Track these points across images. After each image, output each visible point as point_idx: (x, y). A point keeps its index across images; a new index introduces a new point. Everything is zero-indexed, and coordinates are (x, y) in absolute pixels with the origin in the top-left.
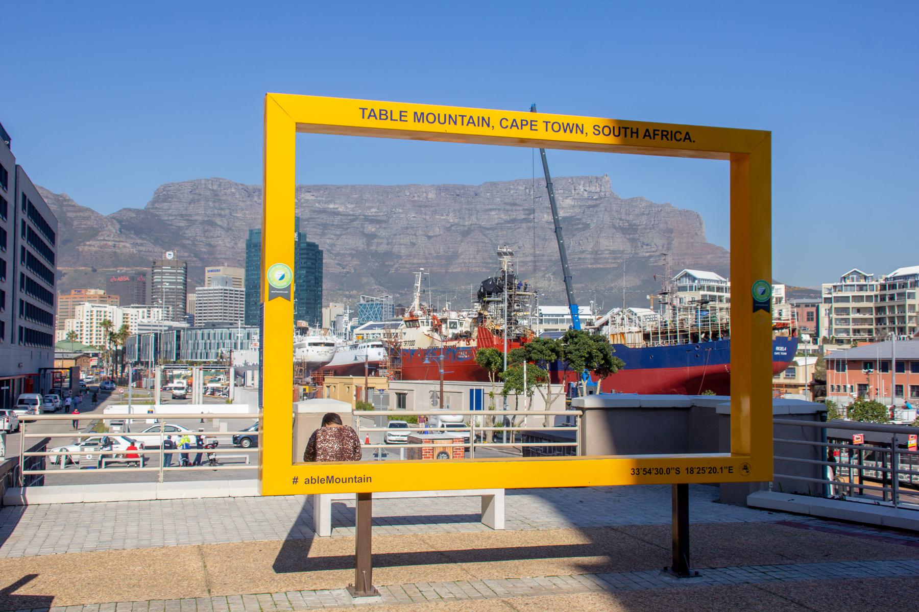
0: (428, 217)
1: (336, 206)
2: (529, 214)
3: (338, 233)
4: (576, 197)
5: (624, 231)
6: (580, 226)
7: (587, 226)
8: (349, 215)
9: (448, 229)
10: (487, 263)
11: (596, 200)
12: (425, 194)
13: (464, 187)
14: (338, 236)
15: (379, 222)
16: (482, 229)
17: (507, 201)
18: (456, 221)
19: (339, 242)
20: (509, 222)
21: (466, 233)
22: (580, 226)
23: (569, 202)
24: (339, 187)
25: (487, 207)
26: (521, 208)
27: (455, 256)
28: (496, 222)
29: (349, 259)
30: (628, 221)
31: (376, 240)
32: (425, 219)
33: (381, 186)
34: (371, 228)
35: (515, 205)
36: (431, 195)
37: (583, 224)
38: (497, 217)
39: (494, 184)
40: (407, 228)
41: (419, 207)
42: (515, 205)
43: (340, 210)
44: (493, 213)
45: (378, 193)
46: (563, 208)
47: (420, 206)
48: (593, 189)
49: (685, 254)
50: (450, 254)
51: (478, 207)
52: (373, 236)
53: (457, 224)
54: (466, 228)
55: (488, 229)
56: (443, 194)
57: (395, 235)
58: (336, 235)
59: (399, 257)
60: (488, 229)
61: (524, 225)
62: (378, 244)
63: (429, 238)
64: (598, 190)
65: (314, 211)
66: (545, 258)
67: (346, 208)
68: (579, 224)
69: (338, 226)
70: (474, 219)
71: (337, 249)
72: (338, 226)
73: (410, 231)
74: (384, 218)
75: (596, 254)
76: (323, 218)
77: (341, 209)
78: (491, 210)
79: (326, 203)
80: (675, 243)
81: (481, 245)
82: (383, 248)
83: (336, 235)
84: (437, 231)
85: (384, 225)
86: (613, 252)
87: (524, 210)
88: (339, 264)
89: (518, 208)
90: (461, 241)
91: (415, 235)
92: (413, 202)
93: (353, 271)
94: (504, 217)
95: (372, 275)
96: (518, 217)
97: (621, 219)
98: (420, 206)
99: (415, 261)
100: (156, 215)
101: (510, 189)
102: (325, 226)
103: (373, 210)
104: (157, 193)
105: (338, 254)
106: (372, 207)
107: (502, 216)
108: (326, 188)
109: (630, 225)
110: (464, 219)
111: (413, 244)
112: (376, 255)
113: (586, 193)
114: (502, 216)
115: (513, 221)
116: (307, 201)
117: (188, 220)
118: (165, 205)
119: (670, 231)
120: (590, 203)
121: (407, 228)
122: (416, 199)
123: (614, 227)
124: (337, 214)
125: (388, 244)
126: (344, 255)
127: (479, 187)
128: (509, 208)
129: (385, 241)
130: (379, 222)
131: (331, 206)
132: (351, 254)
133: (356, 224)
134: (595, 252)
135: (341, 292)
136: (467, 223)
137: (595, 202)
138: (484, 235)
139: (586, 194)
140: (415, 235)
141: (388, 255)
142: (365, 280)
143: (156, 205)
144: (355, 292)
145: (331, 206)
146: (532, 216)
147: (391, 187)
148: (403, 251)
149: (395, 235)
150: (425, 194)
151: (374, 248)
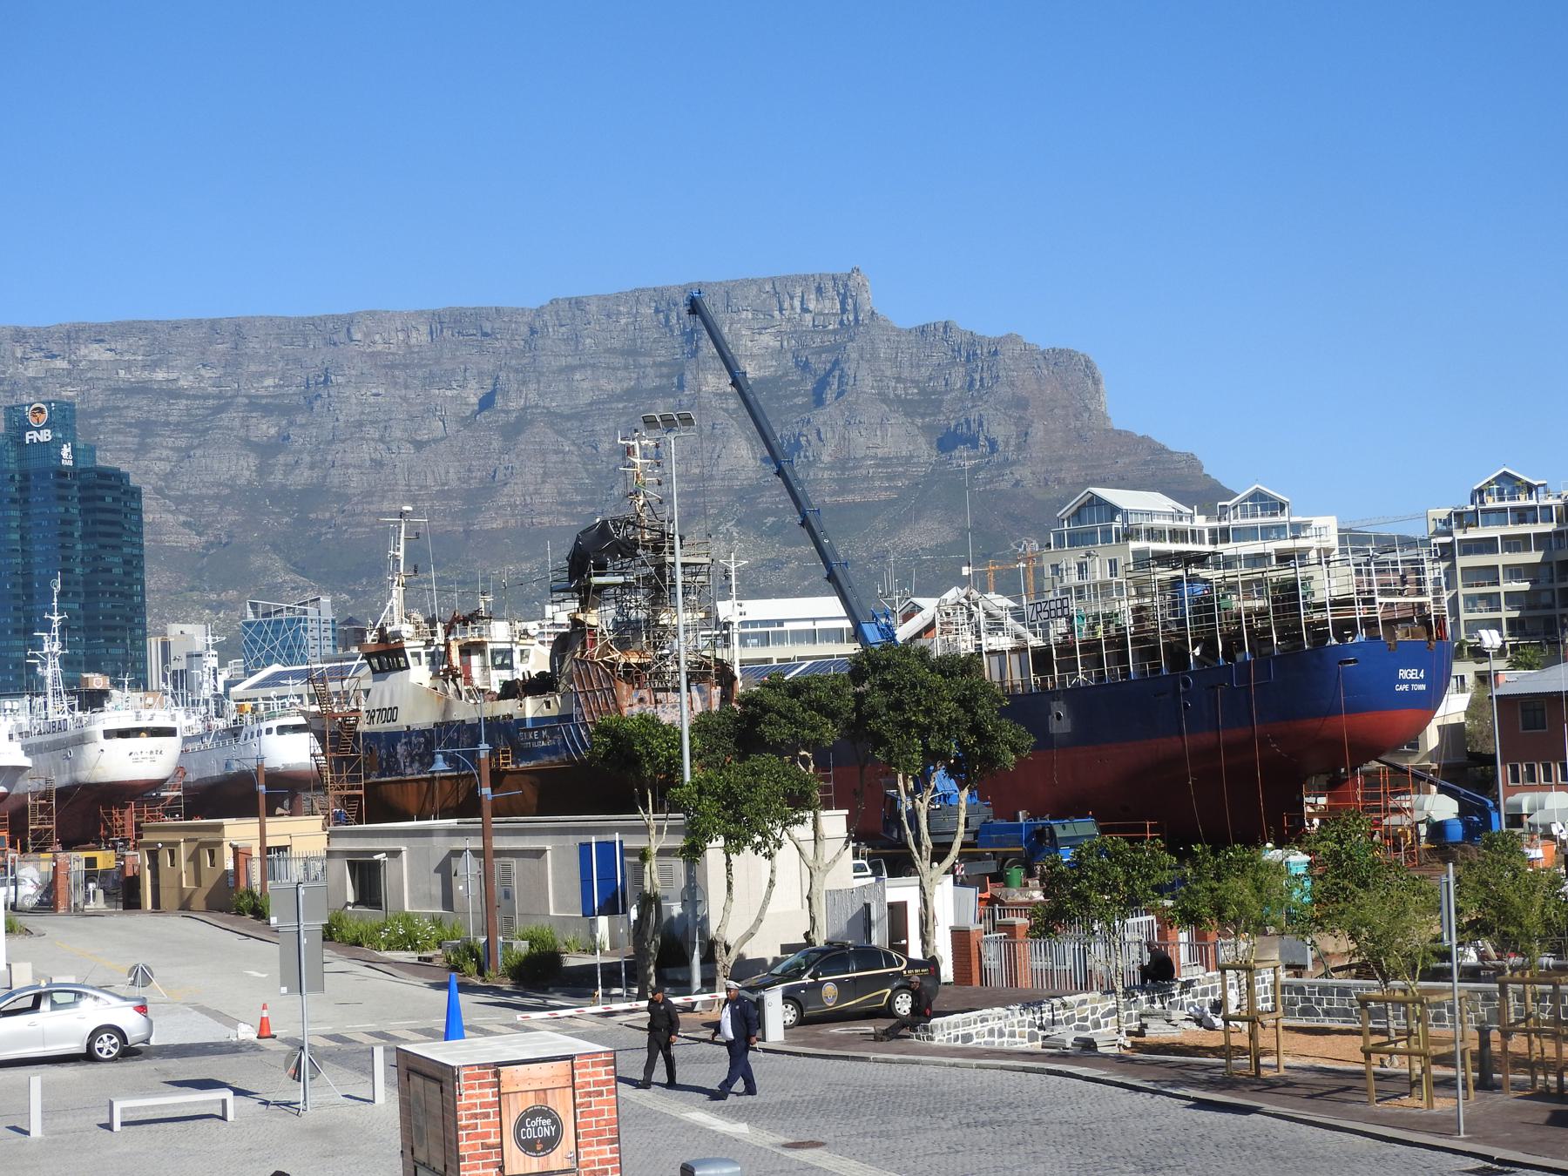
3: (182, 443)
4: (786, 327)
5: (909, 408)
8: (206, 397)
10: (571, 504)
11: (835, 332)
17: (617, 344)
20: (620, 398)
23: (768, 340)
24: (176, 326)
26: (649, 360)
29: (214, 509)
30: (916, 383)
32: (405, 399)
33: (288, 319)
36: (420, 337)
39: (578, 304)
40: (360, 424)
45: (279, 338)
47: (393, 366)
49: (1062, 459)
55: (568, 418)
59: (343, 497)
60: (568, 418)
63: (419, 445)
65: (116, 391)
67: (201, 378)
69: (181, 427)
72: (181, 427)
75: (844, 469)
76: (137, 409)
79: (144, 367)
80: (1038, 432)
81: (554, 458)
82: (303, 477)
86: (885, 462)
92: (373, 355)
94: (609, 385)
95: (275, 548)
97: (898, 379)
98: (393, 366)
99: (386, 506)
101: (619, 313)
102: (146, 428)
103: (269, 382)
105: (180, 500)
106: (263, 375)
108: (144, 328)
109: (922, 392)
111: (378, 464)
112: (280, 496)
116: (94, 365)
119: (1021, 403)
122: (379, 348)
123: (884, 399)
124: (175, 394)
126: (200, 498)
127: (539, 312)
131: (160, 375)
132: (217, 497)
134: (842, 463)
135: (195, 595)
141: (315, 494)
142: (257, 562)
144: (233, 594)
145: (160, 375)
147: (312, 321)
148: (356, 482)
150: (401, 336)
151: (277, 478)
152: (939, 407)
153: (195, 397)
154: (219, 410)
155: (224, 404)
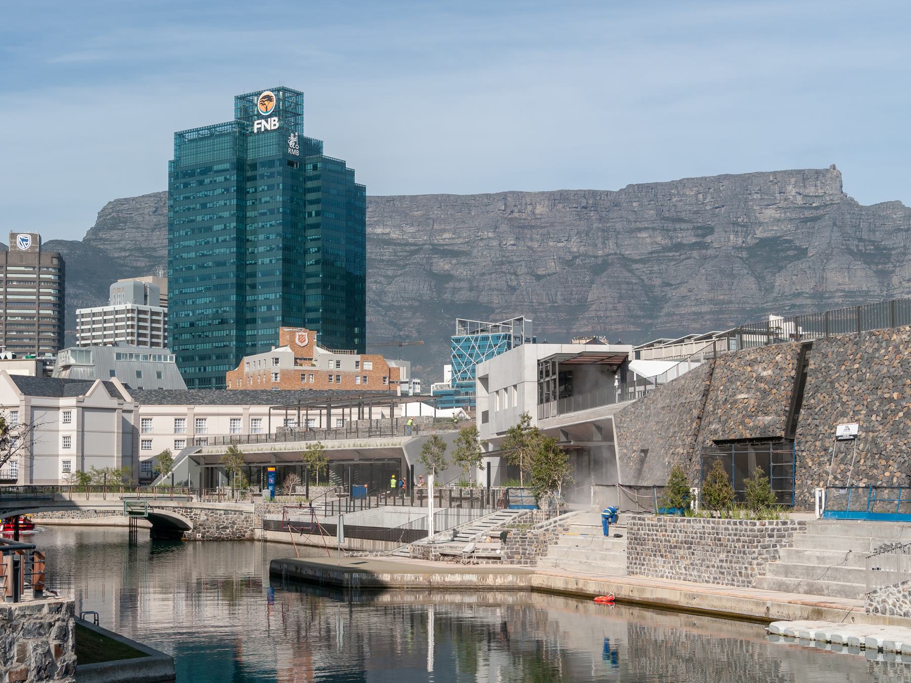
0: (535, 245)
1: (387, 230)
2: (704, 236)
3: (390, 273)
6: (791, 253)
7: (802, 253)
8: (408, 244)
9: (569, 263)
11: (817, 208)
12: (530, 208)
13: (594, 193)
14: (390, 279)
15: (455, 254)
16: (626, 262)
18: (582, 249)
19: (391, 288)
20: (670, 250)
21: (600, 268)
22: (791, 253)
23: (770, 213)
25: (633, 226)
26: (690, 226)
27: (583, 305)
28: (650, 249)
29: (409, 315)
31: (451, 284)
34: (443, 265)
35: (680, 220)
37: (797, 248)
38: (648, 241)
40: (502, 263)
41: (521, 228)
42: (680, 220)
43: (393, 236)
44: (644, 234)
46: (761, 224)
47: (523, 227)
48: (811, 191)
50: (574, 303)
51: (619, 226)
52: (448, 277)
53: (586, 255)
54: (599, 261)
55: (636, 261)
56: (561, 206)
57: (483, 274)
58: (386, 277)
60: (636, 261)
61: (695, 254)
62: (455, 290)
63: (539, 278)
64: (820, 192)
66: (733, 307)
68: (789, 249)
69: (390, 263)
70: (611, 247)
71: (388, 299)
72: (390, 263)
73: (504, 268)
74: (465, 248)
77: (395, 235)
78: (640, 230)
81: (624, 286)
82: (464, 296)
83: (386, 277)
84: (552, 266)
85: (464, 260)
87: (695, 228)
88: (391, 323)
89: (683, 226)
90: (592, 282)
91: (515, 274)
92: (510, 220)
93: (415, 334)
96: (685, 242)
98: (523, 227)
100: (101, 250)
103: (447, 235)
104: (102, 214)
105: (391, 307)
106: (444, 231)
107: (659, 239)
110: (595, 245)
111: (513, 289)
113: (799, 198)
114: (659, 239)
115: (678, 247)
117: (150, 257)
118: (115, 235)
120: (807, 214)
121: (502, 263)
122: (516, 215)
124: (389, 242)
125: (471, 289)
128: (670, 225)
129: (464, 285)
130: (455, 254)
133: (417, 257)
136: (600, 253)
137: (815, 213)
138: (630, 271)
139: (799, 200)
140: (515, 274)
143: (101, 234)
146: (708, 239)
148: (496, 300)
149: (483, 274)
151: (447, 296)
152: (889, 259)
153: (400, 244)
154: (413, 253)
155: (418, 249)
